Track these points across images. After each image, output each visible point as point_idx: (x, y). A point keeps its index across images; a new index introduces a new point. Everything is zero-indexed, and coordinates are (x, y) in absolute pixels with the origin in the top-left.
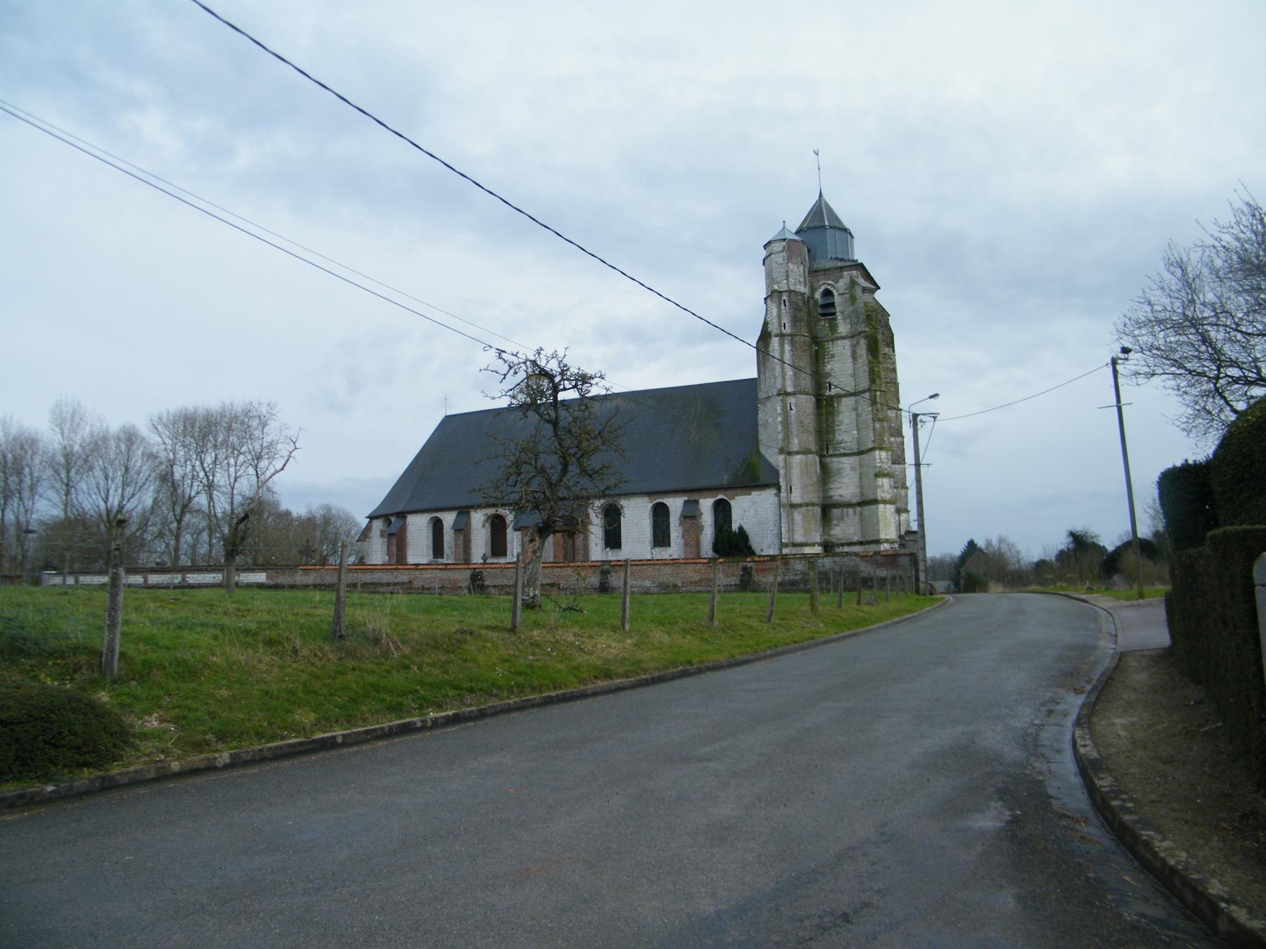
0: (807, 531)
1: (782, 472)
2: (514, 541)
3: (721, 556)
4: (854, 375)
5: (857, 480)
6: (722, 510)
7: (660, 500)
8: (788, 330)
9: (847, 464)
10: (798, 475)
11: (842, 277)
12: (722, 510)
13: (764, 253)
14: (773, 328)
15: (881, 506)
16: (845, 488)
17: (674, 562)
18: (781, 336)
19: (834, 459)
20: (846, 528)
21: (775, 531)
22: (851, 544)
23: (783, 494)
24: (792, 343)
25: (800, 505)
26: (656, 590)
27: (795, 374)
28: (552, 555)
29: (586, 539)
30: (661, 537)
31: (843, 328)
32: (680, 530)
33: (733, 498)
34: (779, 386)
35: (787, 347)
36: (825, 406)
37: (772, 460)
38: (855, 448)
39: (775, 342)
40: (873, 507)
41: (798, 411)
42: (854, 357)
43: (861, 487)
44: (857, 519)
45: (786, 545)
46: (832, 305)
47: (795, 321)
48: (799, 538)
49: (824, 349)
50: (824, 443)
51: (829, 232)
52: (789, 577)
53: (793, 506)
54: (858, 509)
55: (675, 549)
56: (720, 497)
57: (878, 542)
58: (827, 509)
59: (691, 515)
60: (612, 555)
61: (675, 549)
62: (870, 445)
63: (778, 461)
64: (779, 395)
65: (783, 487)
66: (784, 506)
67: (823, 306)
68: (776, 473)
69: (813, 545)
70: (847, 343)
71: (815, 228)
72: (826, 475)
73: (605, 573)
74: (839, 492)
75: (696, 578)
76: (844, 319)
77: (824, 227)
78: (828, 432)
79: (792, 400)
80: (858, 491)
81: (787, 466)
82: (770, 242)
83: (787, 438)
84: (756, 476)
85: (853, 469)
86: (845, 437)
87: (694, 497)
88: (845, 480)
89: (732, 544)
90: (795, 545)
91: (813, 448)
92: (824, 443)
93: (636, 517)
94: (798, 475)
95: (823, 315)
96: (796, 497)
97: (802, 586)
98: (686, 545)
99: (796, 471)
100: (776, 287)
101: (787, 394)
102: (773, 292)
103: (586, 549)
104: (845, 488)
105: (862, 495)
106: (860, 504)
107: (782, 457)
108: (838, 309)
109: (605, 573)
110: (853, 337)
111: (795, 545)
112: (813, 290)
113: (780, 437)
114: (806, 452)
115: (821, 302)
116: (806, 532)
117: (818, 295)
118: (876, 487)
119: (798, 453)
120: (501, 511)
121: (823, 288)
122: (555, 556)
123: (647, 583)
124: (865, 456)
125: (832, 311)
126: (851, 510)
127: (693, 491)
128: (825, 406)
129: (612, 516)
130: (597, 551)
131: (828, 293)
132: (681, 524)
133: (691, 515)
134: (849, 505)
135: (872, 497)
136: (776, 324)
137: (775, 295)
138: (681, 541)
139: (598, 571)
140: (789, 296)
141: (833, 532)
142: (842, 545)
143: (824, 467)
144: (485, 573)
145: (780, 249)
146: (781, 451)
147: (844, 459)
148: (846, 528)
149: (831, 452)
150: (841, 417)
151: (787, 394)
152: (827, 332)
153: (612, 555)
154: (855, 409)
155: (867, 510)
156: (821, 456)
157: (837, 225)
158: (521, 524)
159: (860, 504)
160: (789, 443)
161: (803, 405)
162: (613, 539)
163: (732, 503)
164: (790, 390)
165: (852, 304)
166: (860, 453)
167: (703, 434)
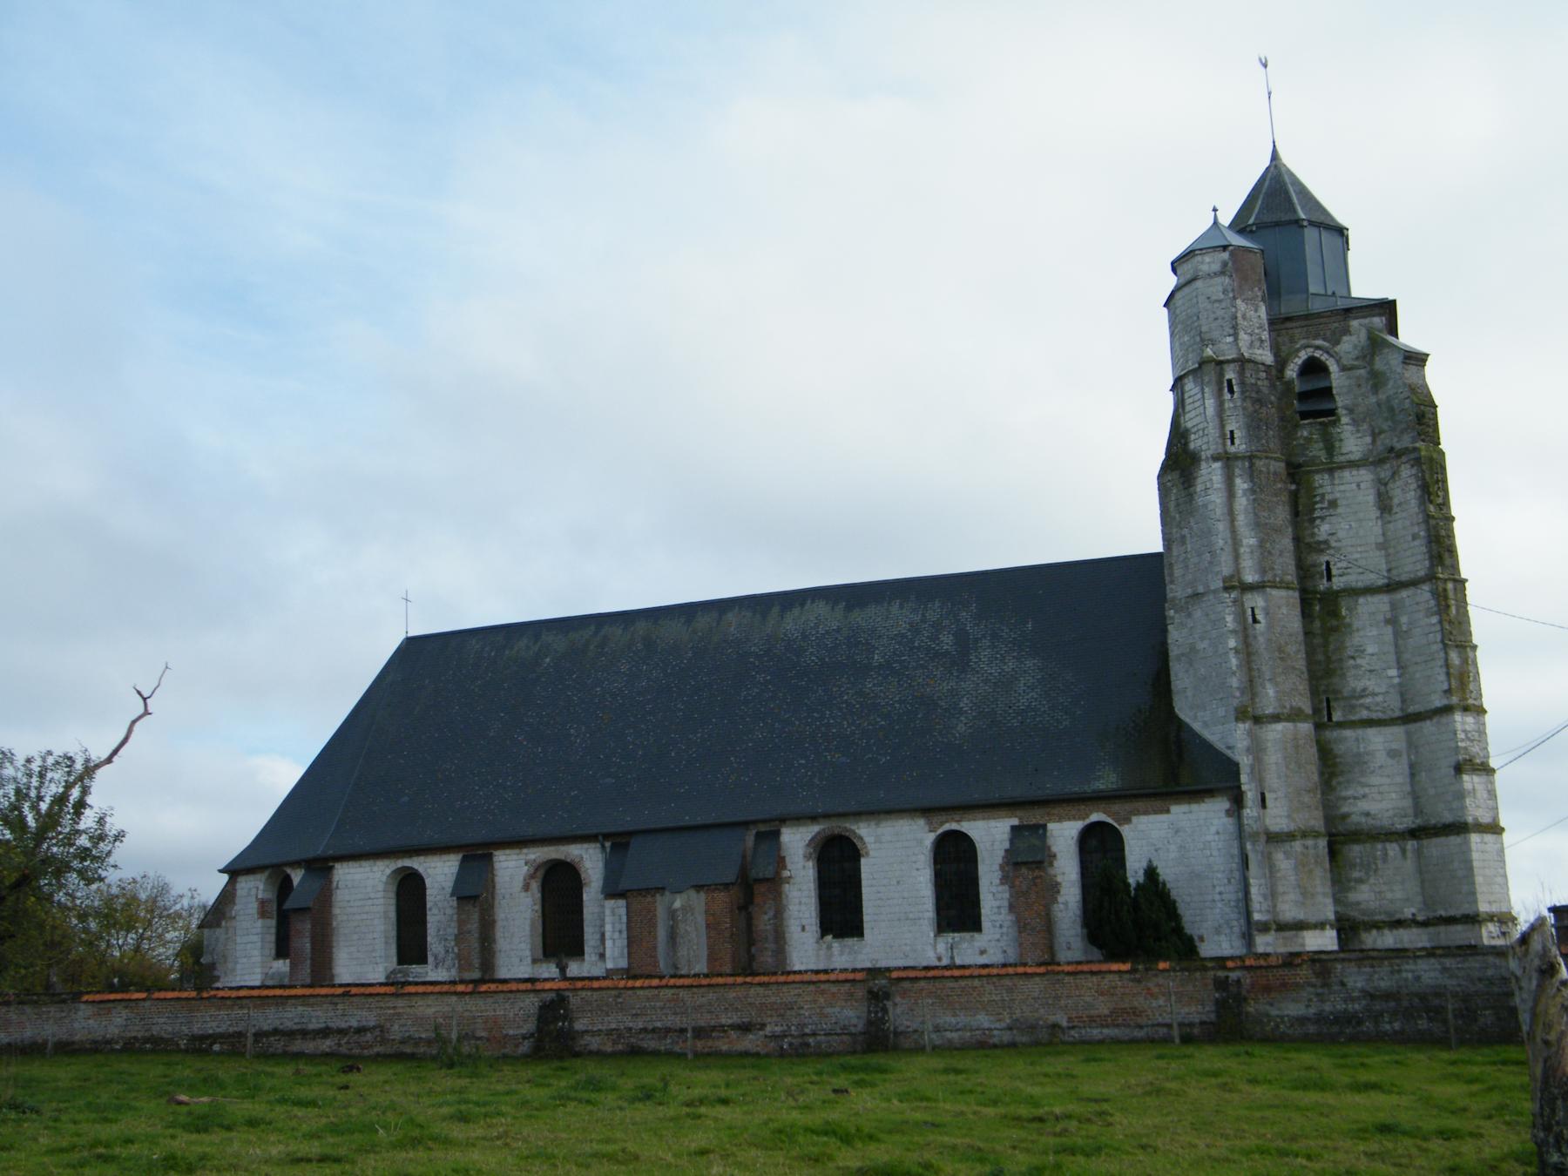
0: (1306, 894)
1: (1245, 761)
2: (606, 926)
3: (1112, 956)
4: (1383, 546)
5: (1402, 779)
6: (1101, 846)
7: (954, 826)
8: (1240, 446)
9: (1378, 741)
10: (1274, 761)
11: (1347, 331)
12: (1101, 846)
13: (1171, 281)
14: (1203, 442)
15: (1475, 838)
16: (1380, 796)
17: (985, 973)
18: (1227, 459)
19: (1348, 733)
20: (1389, 885)
21: (1232, 893)
22: (1398, 924)
23: (1250, 812)
24: (1252, 474)
25: (1289, 837)
26: (1007, 1037)
27: (1261, 544)
28: (704, 953)
29: (779, 914)
30: (957, 906)
31: (1352, 443)
32: (1004, 893)
33: (1128, 820)
34: (1227, 570)
35: (1241, 485)
36: (1322, 607)
37: (1213, 735)
38: (1394, 706)
39: (1211, 475)
40: (1454, 840)
41: (1270, 627)
42: (1385, 505)
43: (1415, 796)
44: (1409, 864)
45: (1264, 928)
46: (1327, 392)
47: (1255, 426)
48: (1289, 910)
49: (1311, 491)
50: (1326, 701)
51: (1310, 234)
52: (1334, 1004)
53: (1274, 838)
54: (1411, 845)
55: (992, 940)
56: (1095, 817)
57: (1473, 919)
58: (1341, 841)
59: (1028, 858)
60: (844, 955)
61: (992, 940)
62: (1438, 702)
63: (1234, 738)
64: (1227, 589)
65: (1250, 796)
66: (1254, 836)
67: (1304, 396)
68: (1232, 769)
69: (1320, 926)
70: (1365, 476)
71: (1277, 224)
72: (1331, 769)
73: (878, 998)
74: (1364, 805)
75: (1103, 1008)
76: (1355, 422)
77: (1297, 222)
78: (1329, 673)
79: (1256, 601)
80: (1407, 803)
81: (1257, 749)
82: (1188, 255)
83: (1251, 686)
84: (1181, 767)
85: (1393, 754)
86: (1371, 683)
87: (1034, 817)
88: (1375, 780)
89: (1135, 920)
90: (1282, 927)
91: (1307, 709)
92: (1326, 701)
93: (896, 860)
94: (1274, 761)
95: (1304, 415)
96: (1278, 817)
97: (1368, 1026)
98: (1022, 926)
99: (1273, 758)
100: (1209, 352)
101: (1247, 588)
102: (1203, 363)
103: (780, 936)
104: (1380, 796)
105: (1418, 810)
106: (1415, 833)
107: (1242, 727)
108: (1341, 401)
109: (878, 998)
110: (1380, 462)
111: (1282, 927)
112: (1281, 363)
113: (1234, 682)
114: (1295, 716)
115: (1298, 387)
116: (1299, 897)
117: (1291, 372)
118: (1461, 795)
119: (1276, 718)
120: (573, 852)
121: (1303, 355)
122: (712, 958)
123: (983, 1020)
124: (1428, 727)
125: (1326, 406)
126: (1393, 849)
127: (1031, 808)
128: (1322, 607)
129: (839, 868)
130: (805, 947)
131: (1313, 368)
132: (1005, 880)
133: (1028, 858)
134: (1388, 835)
135: (1448, 818)
136: (1213, 430)
137: (1210, 373)
138: (1006, 918)
139: (860, 992)
140: (1241, 373)
141: (1353, 897)
142: (1377, 926)
143: (1326, 755)
144: (574, 1001)
145: (1216, 267)
146: (1242, 714)
147: (1371, 732)
148: (1389, 885)
149: (1337, 716)
150: (1356, 639)
151: (1247, 588)
152: (1317, 451)
153: (844, 955)
154: (1392, 621)
155: (1436, 847)
156: (1318, 727)
157: (1322, 219)
158: (624, 884)
159: (1415, 833)
160: (1254, 695)
161: (1279, 612)
162: (842, 912)
163: (1126, 831)
164: (1250, 577)
165: (1376, 388)
166: (1408, 719)
167: (1046, 680)
